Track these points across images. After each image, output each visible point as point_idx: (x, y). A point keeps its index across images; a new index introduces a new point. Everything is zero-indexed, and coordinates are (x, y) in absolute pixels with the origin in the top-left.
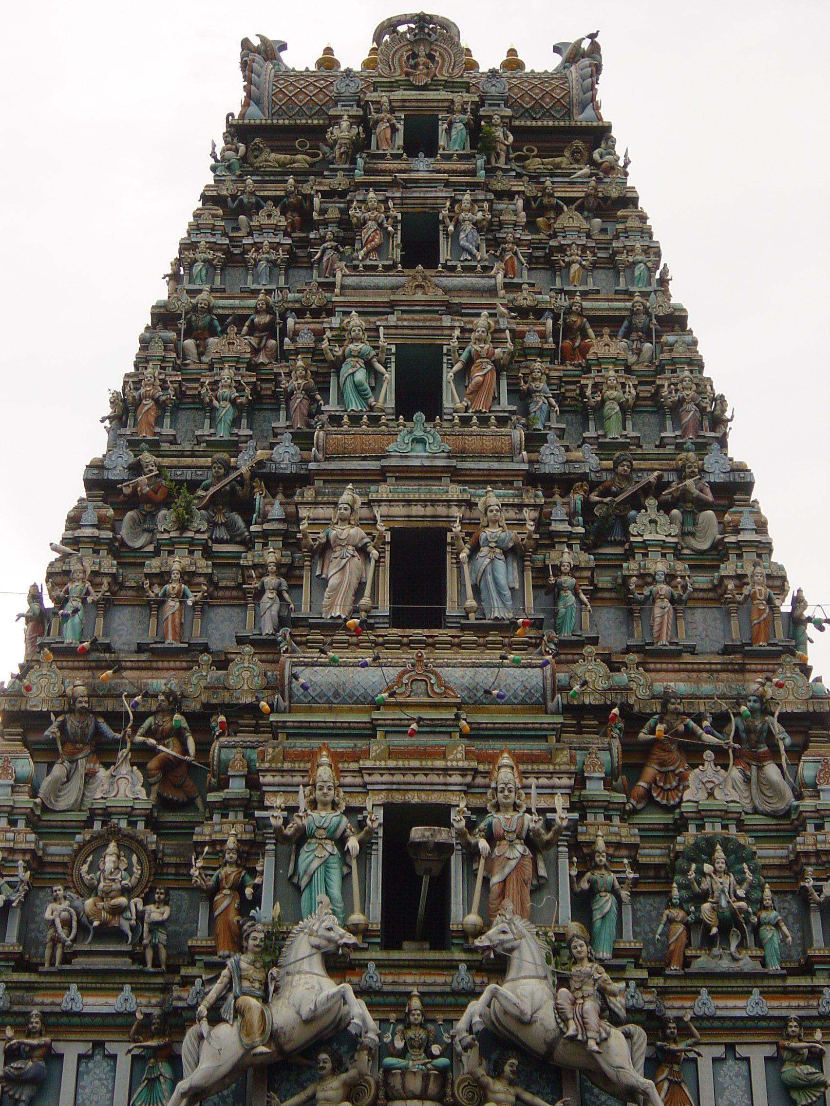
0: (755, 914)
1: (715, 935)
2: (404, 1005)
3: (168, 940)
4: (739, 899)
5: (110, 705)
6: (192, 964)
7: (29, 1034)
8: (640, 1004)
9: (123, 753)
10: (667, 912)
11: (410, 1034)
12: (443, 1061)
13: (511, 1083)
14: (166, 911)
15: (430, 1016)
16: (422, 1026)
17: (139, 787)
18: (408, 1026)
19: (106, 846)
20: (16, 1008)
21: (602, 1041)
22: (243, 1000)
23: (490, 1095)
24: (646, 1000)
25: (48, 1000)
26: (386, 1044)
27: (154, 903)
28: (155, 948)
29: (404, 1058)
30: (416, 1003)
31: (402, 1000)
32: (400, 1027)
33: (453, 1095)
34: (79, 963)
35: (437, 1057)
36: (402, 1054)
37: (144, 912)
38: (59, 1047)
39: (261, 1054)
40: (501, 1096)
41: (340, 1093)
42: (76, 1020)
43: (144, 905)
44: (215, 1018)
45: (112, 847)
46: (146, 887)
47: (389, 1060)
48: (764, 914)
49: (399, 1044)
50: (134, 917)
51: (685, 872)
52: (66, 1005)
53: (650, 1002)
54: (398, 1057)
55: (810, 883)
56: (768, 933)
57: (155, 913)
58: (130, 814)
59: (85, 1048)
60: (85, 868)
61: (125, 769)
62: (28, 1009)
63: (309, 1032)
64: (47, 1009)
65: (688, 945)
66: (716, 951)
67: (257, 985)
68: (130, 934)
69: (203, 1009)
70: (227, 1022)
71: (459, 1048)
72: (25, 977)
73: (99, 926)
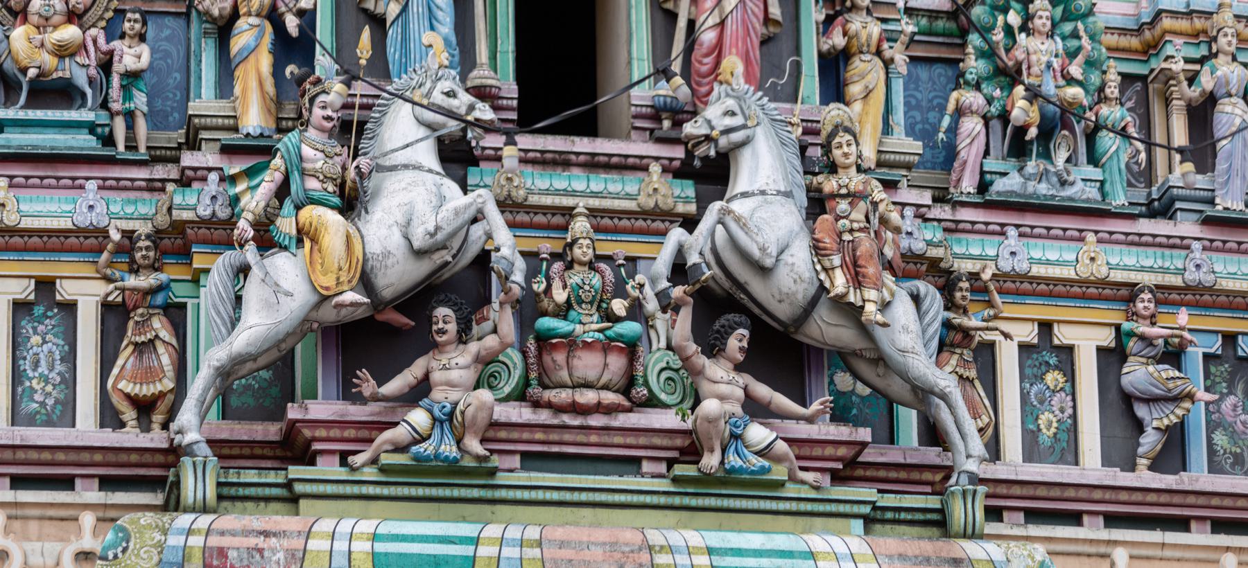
0: (1091, 109)
1: (1031, 142)
2: (565, 228)
3: (149, 104)
4: (1070, 81)
6: (193, 144)
8: (919, 247)
10: (955, 94)
11: (575, 278)
12: (631, 328)
13: (739, 368)
14: (145, 50)
15: (605, 249)
16: (591, 266)
18: (569, 266)
21: (885, 306)
22: (310, 213)
23: (705, 387)
24: (922, 238)
26: (537, 295)
27: (122, 36)
28: (130, 116)
29: (565, 318)
30: (581, 225)
31: (558, 220)
32: (558, 266)
33: (646, 384)
35: (618, 319)
36: (563, 311)
37: (111, 53)
39: (352, 304)
40: (723, 389)
41: (469, 376)
43: (108, 42)
44: (266, 241)
46: (107, 9)
47: (545, 323)
48: (1105, 110)
49: (560, 295)
50: (94, 63)
51: (985, 31)
53: (937, 246)
54: (556, 315)
55: (1178, 66)
56: (1108, 142)
57: (132, 56)
63: (421, 269)
65: (987, 153)
66: (1032, 166)
67: (331, 189)
68: (89, 92)
69: (244, 227)
70: (286, 248)
71: (652, 305)
73: (38, 76)
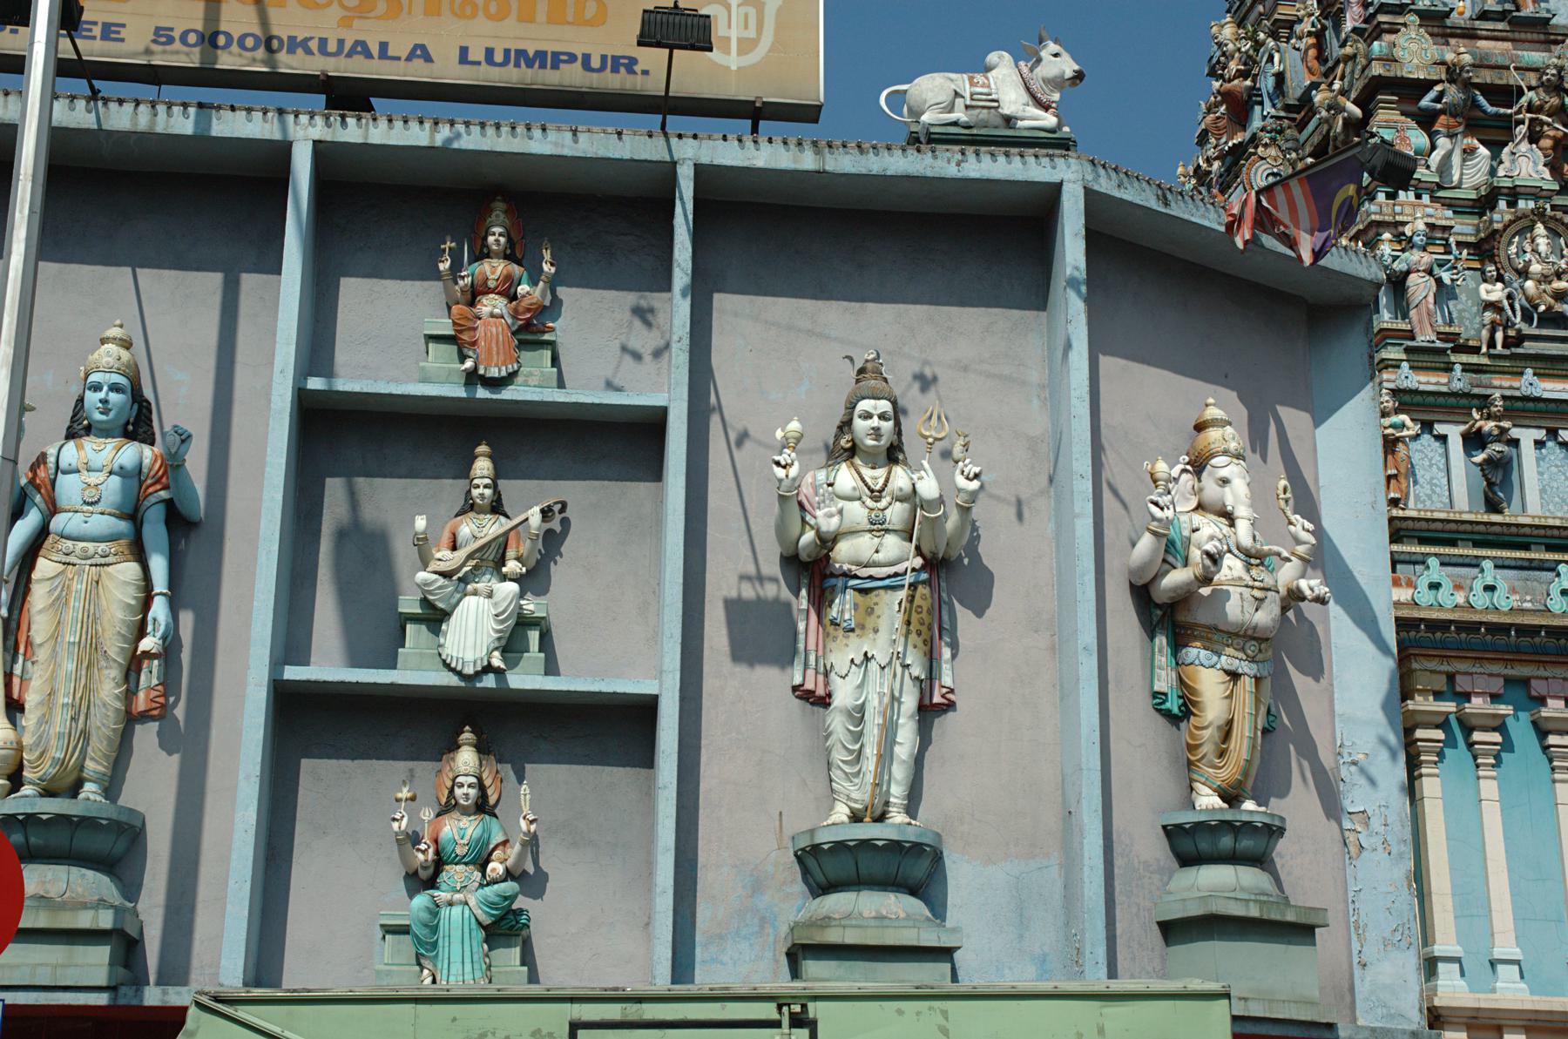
5: (1487, 77)
7: (1489, 417)
9: (1523, 129)
17: (1541, 167)
19: (1532, 228)
20: (1476, 391)
25: (1506, 384)
34: (1530, 347)
38: (1515, 433)
42: (1531, 405)
45: (1540, 229)
52: (1526, 391)
58: (1536, 194)
59: (1540, 434)
60: (1513, 249)
61: (1524, 146)
62: (1489, 392)
64: (1508, 393)
72: (1474, 359)
